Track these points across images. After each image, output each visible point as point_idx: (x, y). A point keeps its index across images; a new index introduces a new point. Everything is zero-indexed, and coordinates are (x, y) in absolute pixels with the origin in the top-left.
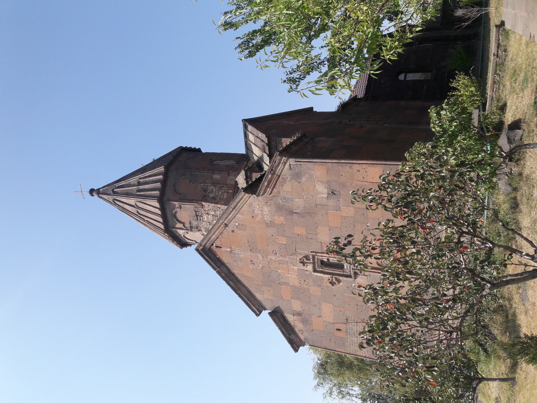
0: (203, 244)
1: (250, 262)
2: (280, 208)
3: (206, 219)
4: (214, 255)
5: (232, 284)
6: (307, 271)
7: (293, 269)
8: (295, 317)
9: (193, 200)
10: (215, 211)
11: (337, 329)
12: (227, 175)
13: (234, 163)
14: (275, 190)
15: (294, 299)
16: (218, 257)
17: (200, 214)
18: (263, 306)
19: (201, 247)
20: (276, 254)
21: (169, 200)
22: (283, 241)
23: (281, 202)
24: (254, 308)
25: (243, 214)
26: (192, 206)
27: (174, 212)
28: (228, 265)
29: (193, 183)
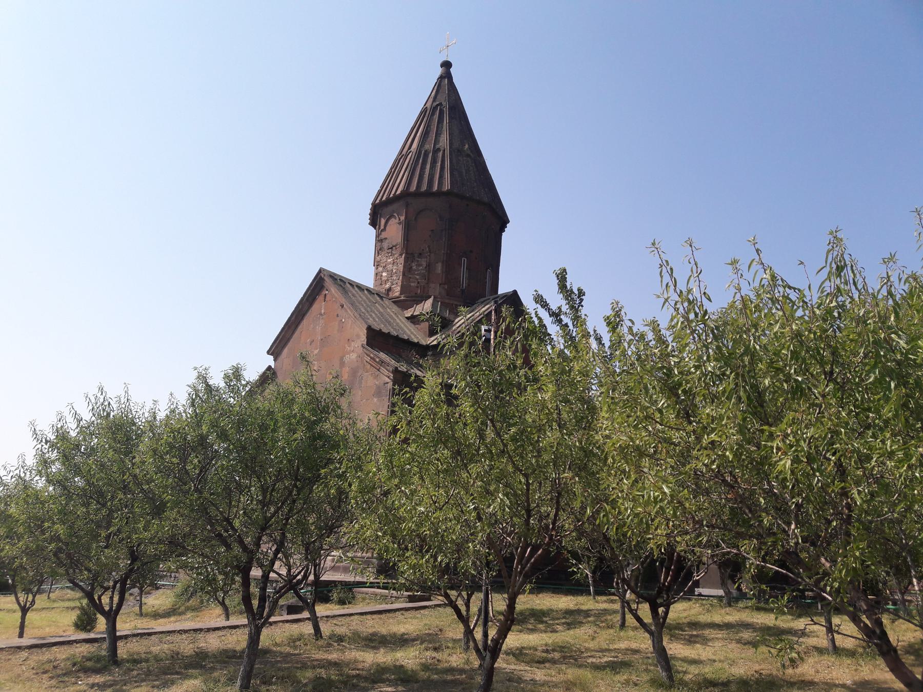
0: (325, 278)
2: (354, 372)
3: (389, 260)
4: (318, 294)
5: (293, 319)
9: (407, 241)
10: (396, 273)
12: (441, 282)
13: (463, 287)
14: (369, 366)
17: (394, 252)
21: (407, 205)
23: (359, 374)
27: (395, 214)
28: (310, 311)
29: (430, 236)
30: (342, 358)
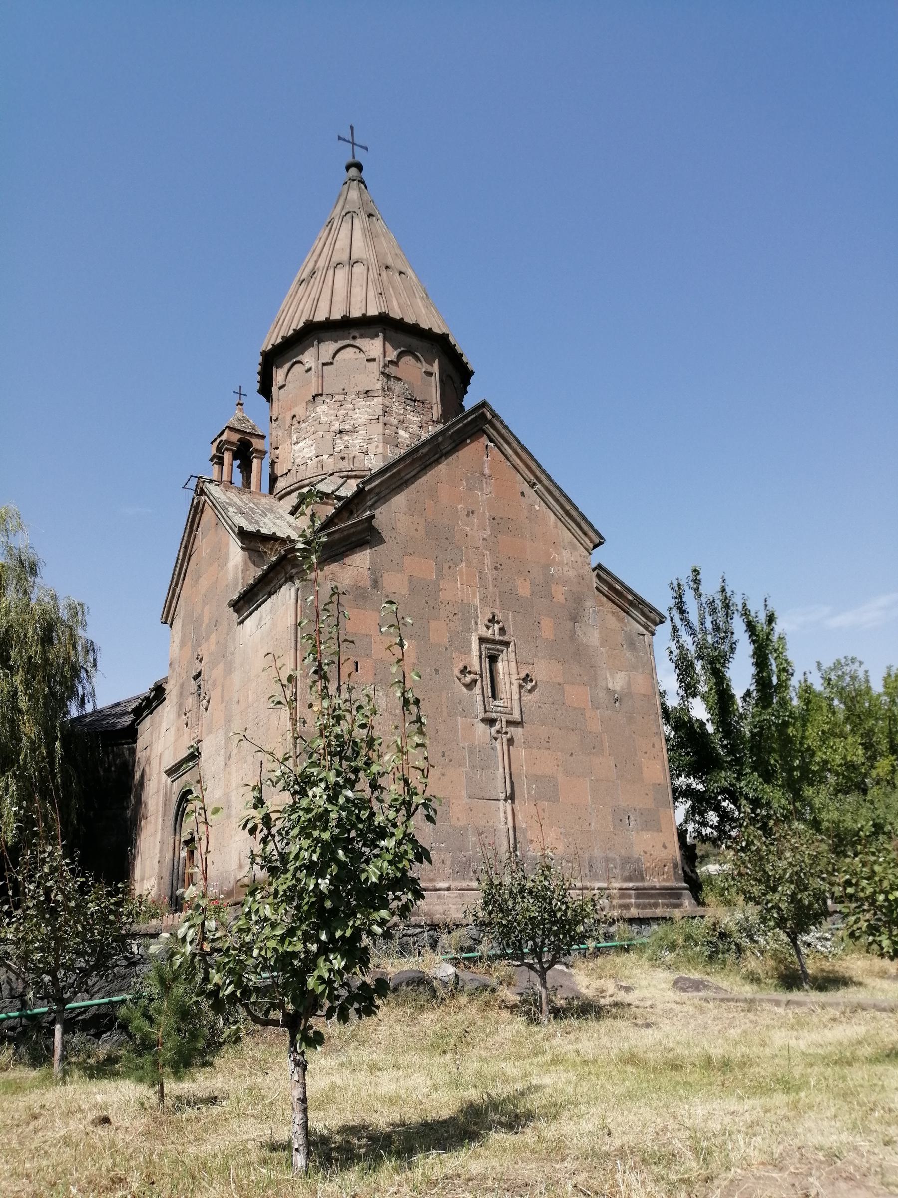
1: (471, 508)
6: (476, 624)
7: (474, 596)
8: (366, 573)
11: (357, 663)
15: (410, 582)
16: (469, 441)
18: (378, 504)
19: (489, 416)
20: (496, 568)
22: (524, 589)
23: (588, 604)
24: (377, 482)
25: (556, 527)
26: (434, 401)
27: (418, 354)
28: (455, 456)
30: (547, 566)
